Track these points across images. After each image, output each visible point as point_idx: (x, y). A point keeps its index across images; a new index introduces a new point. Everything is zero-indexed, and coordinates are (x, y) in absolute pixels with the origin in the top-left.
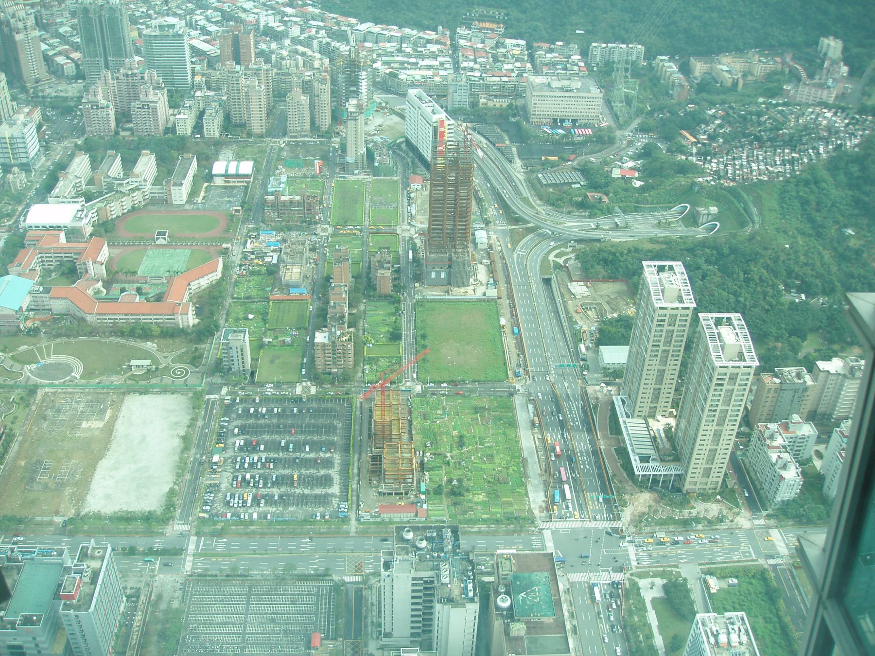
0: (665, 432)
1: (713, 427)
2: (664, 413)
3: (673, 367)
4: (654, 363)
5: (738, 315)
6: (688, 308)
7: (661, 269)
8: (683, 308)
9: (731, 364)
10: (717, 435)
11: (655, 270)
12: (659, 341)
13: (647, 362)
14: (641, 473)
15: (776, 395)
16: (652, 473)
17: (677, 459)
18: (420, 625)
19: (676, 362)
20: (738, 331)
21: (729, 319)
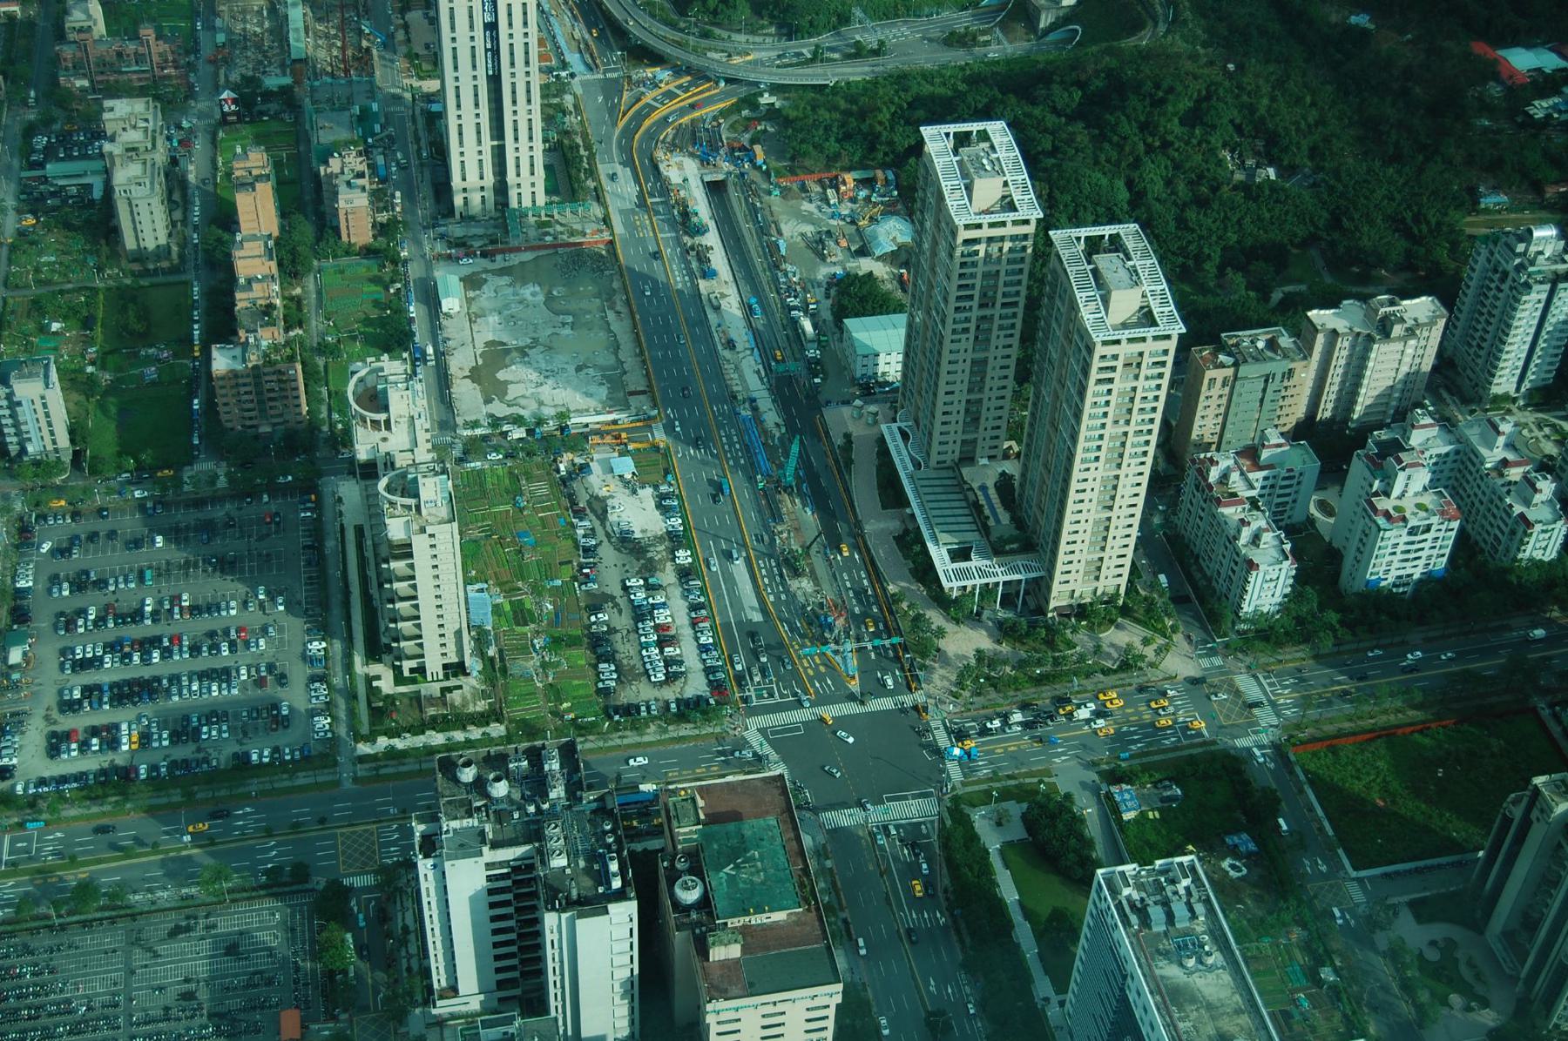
2: (993, 452)
3: (1003, 350)
4: (962, 346)
5: (1134, 227)
7: (962, 140)
9: (1127, 334)
13: (947, 346)
14: (956, 584)
15: (1227, 389)
18: (515, 962)
19: (1009, 341)
20: (1136, 262)
21: (1115, 238)
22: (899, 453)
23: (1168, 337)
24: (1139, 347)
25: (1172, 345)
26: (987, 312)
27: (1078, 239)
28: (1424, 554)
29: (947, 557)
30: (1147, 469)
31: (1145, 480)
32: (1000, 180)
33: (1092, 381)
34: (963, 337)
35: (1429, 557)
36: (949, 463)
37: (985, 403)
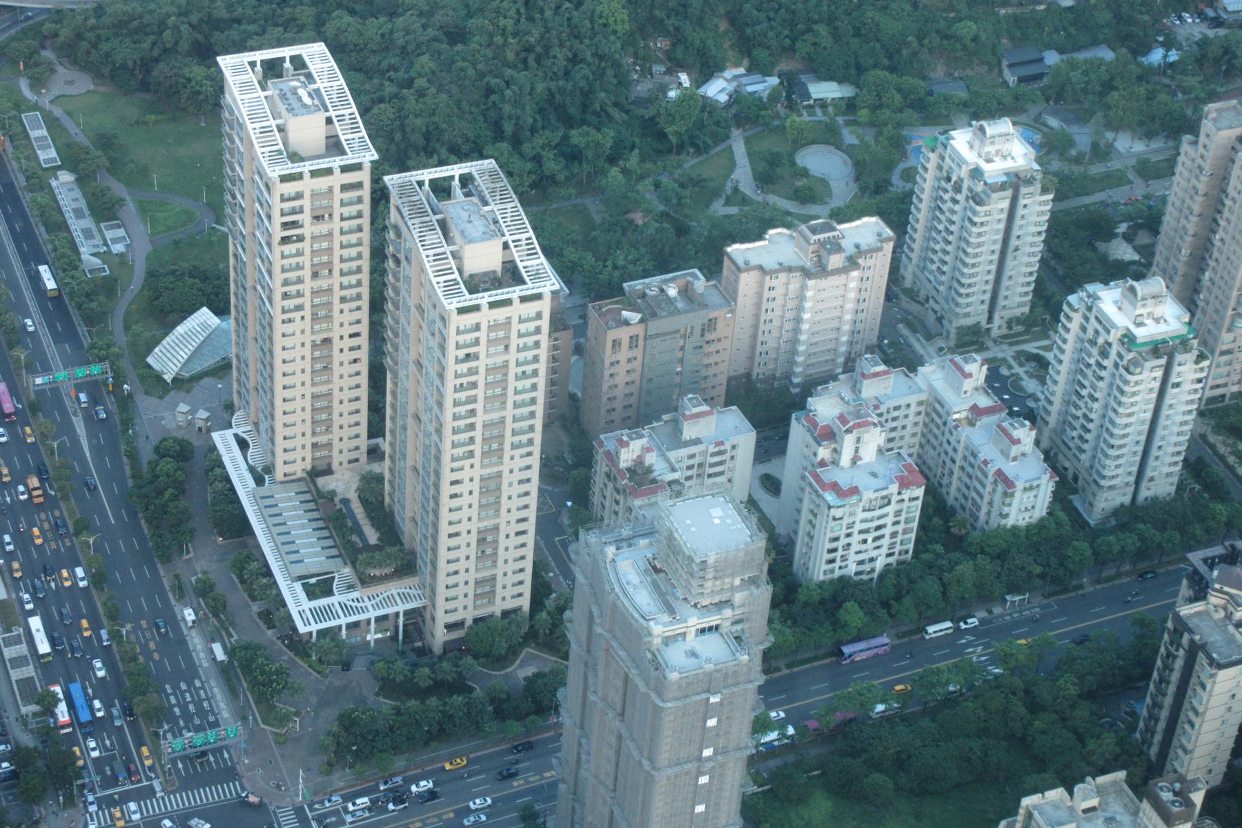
0: (364, 502)
1: (473, 473)
4: (297, 326)
5: (489, 164)
6: (358, 167)
7: (272, 69)
8: (345, 169)
9: (484, 298)
10: (491, 487)
11: (252, 77)
12: (299, 267)
13: (279, 328)
14: (314, 628)
15: (638, 352)
16: (343, 621)
17: (407, 567)
21: (466, 180)
22: (237, 468)
23: (538, 297)
24: (501, 314)
25: (545, 306)
26: (323, 284)
27: (420, 184)
28: (887, 531)
29: (302, 595)
30: (535, 461)
31: (534, 474)
32: (322, 116)
33: (451, 360)
34: (297, 315)
35: (894, 535)
36: (300, 474)
37: (337, 396)
